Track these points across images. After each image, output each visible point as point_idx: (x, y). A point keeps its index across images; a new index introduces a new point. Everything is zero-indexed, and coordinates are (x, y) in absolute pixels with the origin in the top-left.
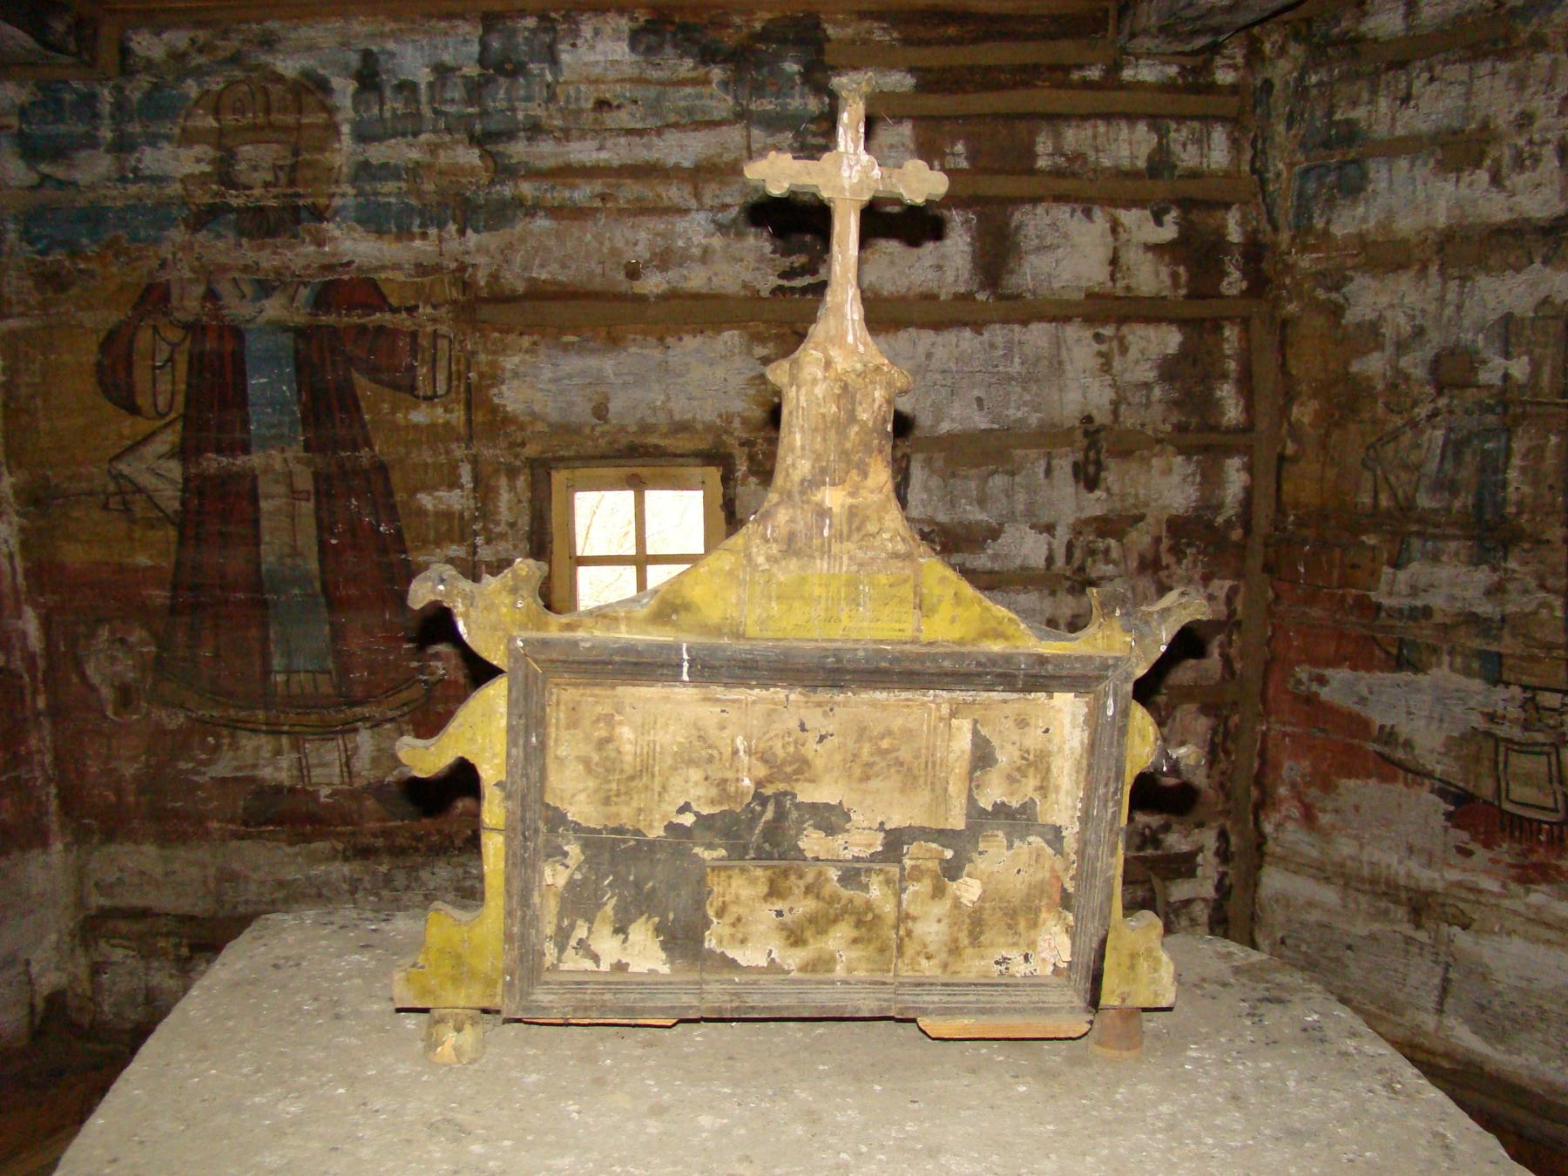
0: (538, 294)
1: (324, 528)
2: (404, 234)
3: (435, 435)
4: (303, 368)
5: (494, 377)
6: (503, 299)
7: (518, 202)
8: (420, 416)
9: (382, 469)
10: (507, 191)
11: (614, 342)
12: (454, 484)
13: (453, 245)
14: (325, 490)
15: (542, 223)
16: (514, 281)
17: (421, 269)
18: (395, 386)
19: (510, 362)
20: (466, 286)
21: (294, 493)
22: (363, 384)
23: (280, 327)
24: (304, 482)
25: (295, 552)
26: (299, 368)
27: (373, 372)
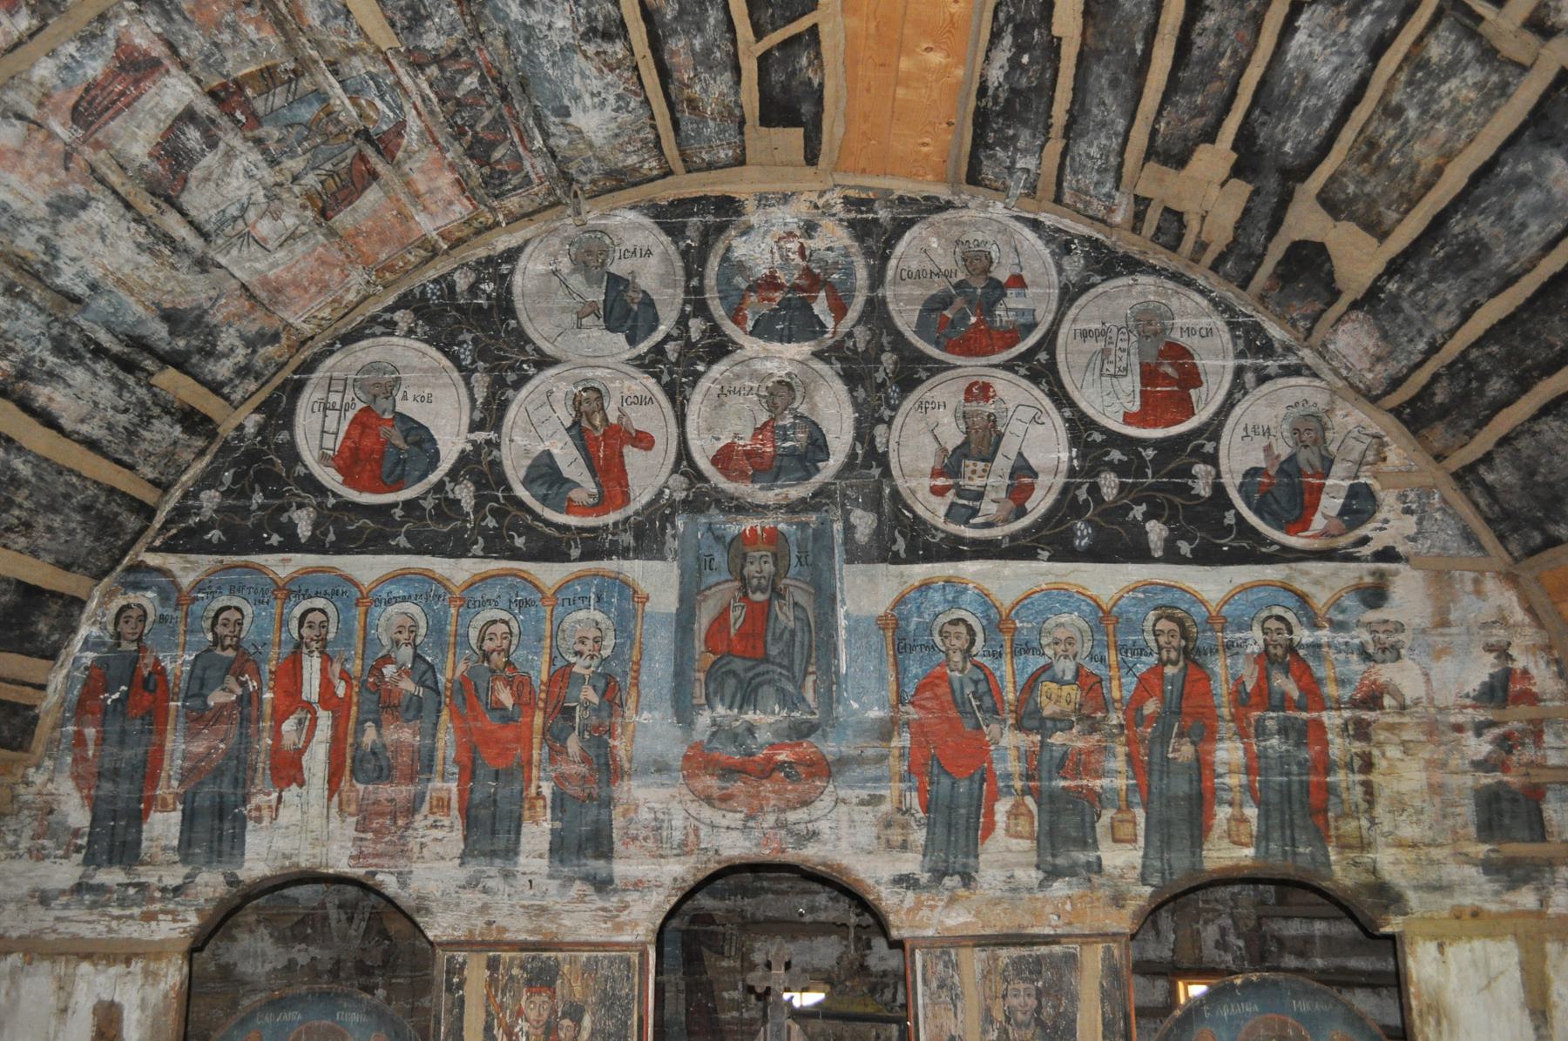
0: (769, 921)
1: (688, 1003)
2: (723, 898)
3: (730, 970)
4: (685, 946)
5: (752, 950)
6: (756, 922)
7: (762, 888)
8: (725, 964)
9: (710, 983)
10: (758, 884)
11: (794, 938)
12: (736, 989)
13: (740, 903)
14: (690, 990)
15: (770, 896)
16: (760, 915)
17: (728, 911)
18: (716, 952)
19: (758, 945)
20: (743, 917)
21: (678, 991)
22: (706, 953)
23: (678, 930)
24: (682, 986)
25: (677, 1012)
26: (683, 944)
27: (709, 947)
